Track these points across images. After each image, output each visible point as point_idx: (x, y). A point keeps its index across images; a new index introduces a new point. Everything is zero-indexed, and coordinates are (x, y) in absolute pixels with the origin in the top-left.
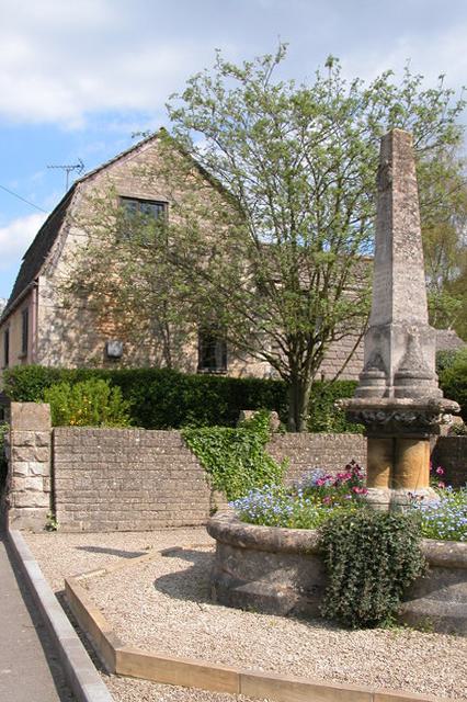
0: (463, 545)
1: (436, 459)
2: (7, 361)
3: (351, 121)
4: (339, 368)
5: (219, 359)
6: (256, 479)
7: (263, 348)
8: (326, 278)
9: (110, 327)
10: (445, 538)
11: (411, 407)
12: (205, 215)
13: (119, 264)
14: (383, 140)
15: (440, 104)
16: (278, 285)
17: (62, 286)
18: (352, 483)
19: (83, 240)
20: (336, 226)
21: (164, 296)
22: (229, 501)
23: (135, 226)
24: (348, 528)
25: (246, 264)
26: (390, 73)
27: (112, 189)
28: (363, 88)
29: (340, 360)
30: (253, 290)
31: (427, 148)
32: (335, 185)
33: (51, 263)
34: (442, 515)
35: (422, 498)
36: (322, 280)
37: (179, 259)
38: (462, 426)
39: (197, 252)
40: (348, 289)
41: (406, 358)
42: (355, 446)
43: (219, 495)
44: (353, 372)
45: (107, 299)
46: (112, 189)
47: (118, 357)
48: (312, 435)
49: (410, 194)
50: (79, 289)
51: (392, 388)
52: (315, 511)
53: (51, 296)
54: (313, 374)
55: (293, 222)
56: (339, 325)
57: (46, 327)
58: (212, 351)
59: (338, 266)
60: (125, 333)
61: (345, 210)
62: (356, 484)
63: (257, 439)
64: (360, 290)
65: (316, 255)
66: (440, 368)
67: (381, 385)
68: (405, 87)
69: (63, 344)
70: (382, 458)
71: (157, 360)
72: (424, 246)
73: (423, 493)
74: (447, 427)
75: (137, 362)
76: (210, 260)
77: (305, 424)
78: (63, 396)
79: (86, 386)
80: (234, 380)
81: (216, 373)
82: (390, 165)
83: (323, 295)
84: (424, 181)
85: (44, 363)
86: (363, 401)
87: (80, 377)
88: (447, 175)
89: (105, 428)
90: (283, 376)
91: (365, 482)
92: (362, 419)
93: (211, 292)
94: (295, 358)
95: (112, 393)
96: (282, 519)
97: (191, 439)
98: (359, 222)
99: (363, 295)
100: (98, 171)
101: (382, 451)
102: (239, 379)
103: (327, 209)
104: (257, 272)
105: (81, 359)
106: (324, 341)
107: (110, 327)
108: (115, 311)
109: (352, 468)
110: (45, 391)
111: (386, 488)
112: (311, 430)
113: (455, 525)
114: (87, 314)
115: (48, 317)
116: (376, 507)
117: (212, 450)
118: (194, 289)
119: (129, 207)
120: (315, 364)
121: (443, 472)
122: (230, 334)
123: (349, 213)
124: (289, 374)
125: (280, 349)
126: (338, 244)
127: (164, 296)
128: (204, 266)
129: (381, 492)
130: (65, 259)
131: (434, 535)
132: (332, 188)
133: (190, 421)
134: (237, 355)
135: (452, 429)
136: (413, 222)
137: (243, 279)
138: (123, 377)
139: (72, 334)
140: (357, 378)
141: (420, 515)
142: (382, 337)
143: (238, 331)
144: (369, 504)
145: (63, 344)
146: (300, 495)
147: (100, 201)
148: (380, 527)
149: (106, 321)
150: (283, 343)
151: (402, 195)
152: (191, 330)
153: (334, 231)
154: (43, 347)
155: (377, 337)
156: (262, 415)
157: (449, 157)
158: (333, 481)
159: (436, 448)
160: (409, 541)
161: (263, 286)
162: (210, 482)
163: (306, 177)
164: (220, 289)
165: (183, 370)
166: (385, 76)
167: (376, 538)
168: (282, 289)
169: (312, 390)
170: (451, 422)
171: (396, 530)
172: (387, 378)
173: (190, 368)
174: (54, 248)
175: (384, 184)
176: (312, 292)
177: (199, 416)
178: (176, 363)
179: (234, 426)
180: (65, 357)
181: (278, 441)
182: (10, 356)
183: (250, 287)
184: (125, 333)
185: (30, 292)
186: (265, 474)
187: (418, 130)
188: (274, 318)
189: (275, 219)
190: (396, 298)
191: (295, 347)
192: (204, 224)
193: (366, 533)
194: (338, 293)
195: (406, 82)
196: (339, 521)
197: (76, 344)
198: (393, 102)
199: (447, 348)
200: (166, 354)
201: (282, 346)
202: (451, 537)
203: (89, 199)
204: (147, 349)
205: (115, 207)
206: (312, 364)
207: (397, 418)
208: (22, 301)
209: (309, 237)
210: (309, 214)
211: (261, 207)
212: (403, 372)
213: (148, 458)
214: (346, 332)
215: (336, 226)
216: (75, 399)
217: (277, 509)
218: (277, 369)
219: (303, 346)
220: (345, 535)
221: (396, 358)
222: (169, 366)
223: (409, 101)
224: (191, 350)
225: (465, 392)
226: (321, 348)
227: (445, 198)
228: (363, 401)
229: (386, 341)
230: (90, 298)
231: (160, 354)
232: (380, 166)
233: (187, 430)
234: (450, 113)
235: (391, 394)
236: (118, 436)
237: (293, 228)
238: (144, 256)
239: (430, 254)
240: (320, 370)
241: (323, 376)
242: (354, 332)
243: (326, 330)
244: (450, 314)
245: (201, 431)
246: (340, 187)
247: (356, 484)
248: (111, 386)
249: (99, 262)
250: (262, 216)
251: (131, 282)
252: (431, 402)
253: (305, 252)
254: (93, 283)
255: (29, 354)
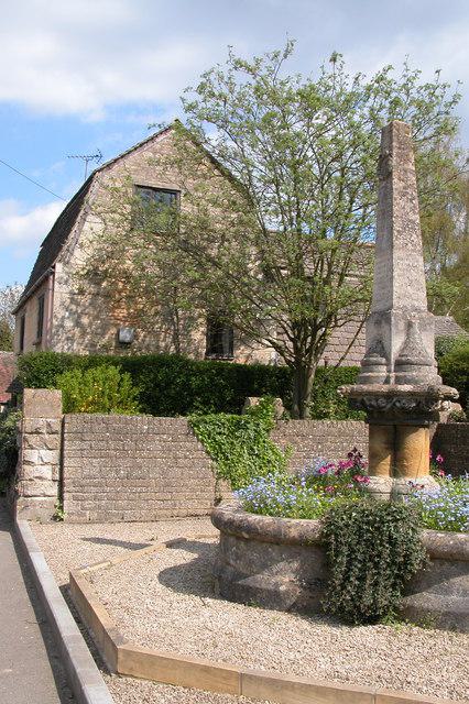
0: (464, 537)
1: (436, 446)
2: (22, 348)
3: (353, 113)
4: (342, 355)
5: (226, 349)
6: (261, 468)
7: (268, 334)
8: (330, 265)
9: (122, 313)
10: (446, 528)
11: (411, 394)
12: (215, 203)
13: (133, 251)
14: (383, 131)
15: (437, 97)
16: (284, 272)
17: (77, 273)
18: (354, 472)
19: (99, 228)
20: (340, 214)
21: (175, 283)
22: (233, 490)
23: (149, 214)
24: (350, 518)
25: (253, 250)
26: (390, 68)
27: (128, 178)
28: (364, 82)
29: (342, 347)
30: (260, 276)
31: (425, 139)
32: (338, 174)
33: (68, 250)
34: (442, 504)
35: (423, 486)
36: (326, 267)
37: (190, 246)
38: (461, 413)
39: (207, 239)
40: (350, 275)
41: (406, 344)
42: (356, 433)
43: (224, 484)
44: (355, 359)
45: (120, 285)
46: (128, 178)
47: (130, 343)
48: (316, 422)
49: (409, 183)
50: (94, 275)
51: (393, 374)
52: (317, 500)
53: (66, 282)
54: (317, 360)
55: (298, 210)
56: (342, 311)
57: (60, 313)
58: (219, 337)
59: (341, 253)
60: (136, 319)
61: (348, 198)
62: (358, 473)
63: (262, 426)
64: (362, 277)
65: (321, 242)
66: (439, 354)
67: (382, 372)
68: (404, 81)
69: (77, 330)
70: (383, 445)
71: (167, 346)
72: (423, 234)
73: (424, 483)
74: (446, 414)
75: (147, 348)
76: (219, 247)
77: (308, 411)
78: (74, 382)
79: (97, 372)
80: (240, 366)
81: (223, 360)
82: (390, 155)
83: (327, 282)
84: (423, 171)
85: (58, 349)
86: (365, 387)
87: (92, 363)
88: (444, 165)
89: (114, 415)
90: (288, 362)
91: (367, 470)
92: (363, 406)
93: (220, 278)
94: (299, 344)
95: (122, 380)
96: (285, 509)
97: (198, 426)
98: (361, 210)
99: (365, 281)
100: (116, 161)
101: (383, 439)
102: (245, 366)
103: (331, 197)
104: (263, 259)
105: (93, 345)
106: (326, 328)
107: (122, 313)
108: (128, 297)
109: (354, 455)
110: (58, 378)
111: (388, 477)
112: (314, 417)
113: (455, 515)
114: (100, 300)
115: (63, 303)
116: (377, 497)
117: (218, 438)
118: (203, 276)
119: (143, 195)
120: (319, 350)
121: (443, 461)
122: (237, 320)
123: (352, 202)
124: (293, 360)
125: (285, 336)
126: (341, 231)
127: (175, 283)
128: (213, 253)
129: (382, 481)
130: (81, 246)
131: (434, 526)
132: (336, 178)
133: (197, 408)
134: (243, 341)
135: (451, 416)
136: (412, 210)
137: (250, 265)
138: (134, 364)
139: (85, 320)
140: (359, 365)
141: (420, 505)
142: (383, 324)
143: (245, 317)
144: (371, 493)
145: (77, 330)
146: (303, 484)
147: (116, 190)
148: (381, 517)
149: (119, 307)
150: (288, 329)
151: (402, 184)
152: (200, 316)
153: (337, 219)
154: (57, 334)
155: (378, 323)
156: (268, 402)
157: (446, 148)
158: (335, 469)
159: (436, 435)
160: (410, 531)
161: (269, 273)
162: (215, 471)
163: (311, 166)
164: (228, 276)
165: (192, 357)
166: (385, 71)
167: (378, 529)
168: (287, 275)
169: (316, 376)
170: (449, 409)
171: (397, 520)
172: (388, 364)
173: (198, 354)
174: (72, 235)
175: (385, 174)
176: (317, 279)
177: (206, 403)
178: (185, 349)
179: (239, 413)
180: (78, 344)
181: (282, 429)
182: (25, 342)
183: (257, 274)
184: (136, 319)
185: (47, 278)
186: (269, 462)
187: (416, 121)
188: (280, 304)
189: (281, 207)
190: (396, 284)
191: (299, 333)
192: (215, 212)
193: (368, 523)
194: (341, 280)
195: (405, 76)
196: (341, 511)
197: (89, 330)
198: (393, 95)
199: (445, 334)
200: (175, 340)
201: (286, 332)
202: (452, 528)
203: (106, 187)
204: (157, 335)
205: (130, 195)
206: (316, 350)
207: (398, 404)
208: (38, 287)
209: (314, 224)
210: (314, 202)
211: (268, 195)
212: (403, 359)
213: (155, 445)
214: (348, 318)
215: (340, 214)
216: (85, 385)
217: (280, 498)
218: (282, 355)
219: (307, 333)
220: (347, 526)
221: (396, 344)
222: (178, 352)
223: (408, 94)
224: (199, 336)
225: (465, 379)
226: (324, 334)
227: (442, 187)
228: (365, 387)
229: (387, 327)
230: (104, 284)
231: (169, 340)
232: (381, 156)
233: (193, 417)
234: (446, 106)
235: (392, 381)
236: (126, 423)
237: (298, 216)
238: (156, 244)
239: (429, 240)
240: (323, 356)
241: (326, 363)
242: (356, 318)
243: (330, 316)
244: (448, 300)
245: (207, 418)
246: (343, 176)
247: (358, 473)
248: (121, 372)
249: (114, 249)
250: (269, 205)
251: (143, 269)
252: (431, 388)
253: (310, 240)
254: (107, 270)
255: (43, 341)
